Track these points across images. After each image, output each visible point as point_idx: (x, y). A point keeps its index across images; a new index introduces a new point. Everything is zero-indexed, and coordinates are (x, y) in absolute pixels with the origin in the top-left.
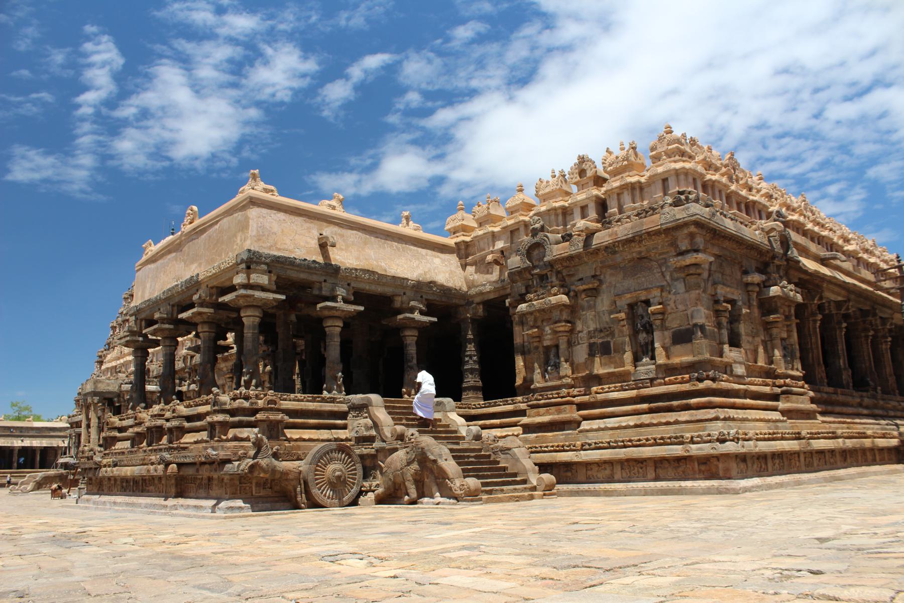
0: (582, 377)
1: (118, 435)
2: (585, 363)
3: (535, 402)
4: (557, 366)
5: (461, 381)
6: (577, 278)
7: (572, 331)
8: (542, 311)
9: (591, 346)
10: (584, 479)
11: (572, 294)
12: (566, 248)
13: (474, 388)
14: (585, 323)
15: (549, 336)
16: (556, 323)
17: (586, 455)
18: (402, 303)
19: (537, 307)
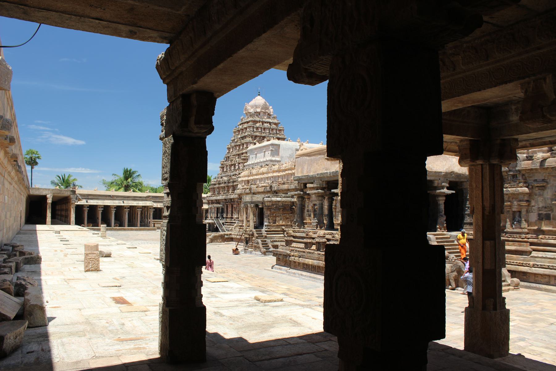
0: (534, 229)
1: (293, 239)
2: (535, 222)
3: (507, 238)
4: (520, 222)
5: (463, 218)
6: (533, 179)
7: (529, 205)
8: (513, 194)
9: (539, 215)
10: (533, 281)
11: (530, 187)
12: (528, 164)
13: (471, 224)
14: (537, 202)
15: (516, 207)
16: (520, 201)
17: (535, 270)
18: (438, 184)
19: (511, 192)
